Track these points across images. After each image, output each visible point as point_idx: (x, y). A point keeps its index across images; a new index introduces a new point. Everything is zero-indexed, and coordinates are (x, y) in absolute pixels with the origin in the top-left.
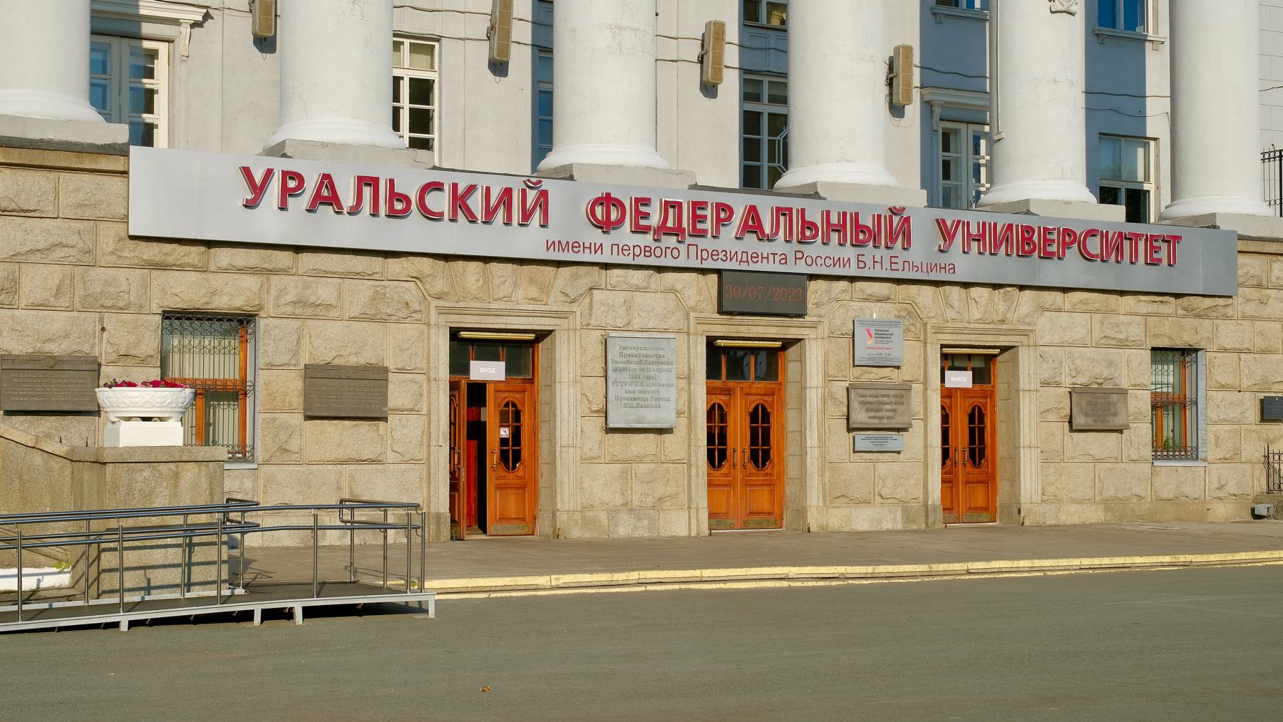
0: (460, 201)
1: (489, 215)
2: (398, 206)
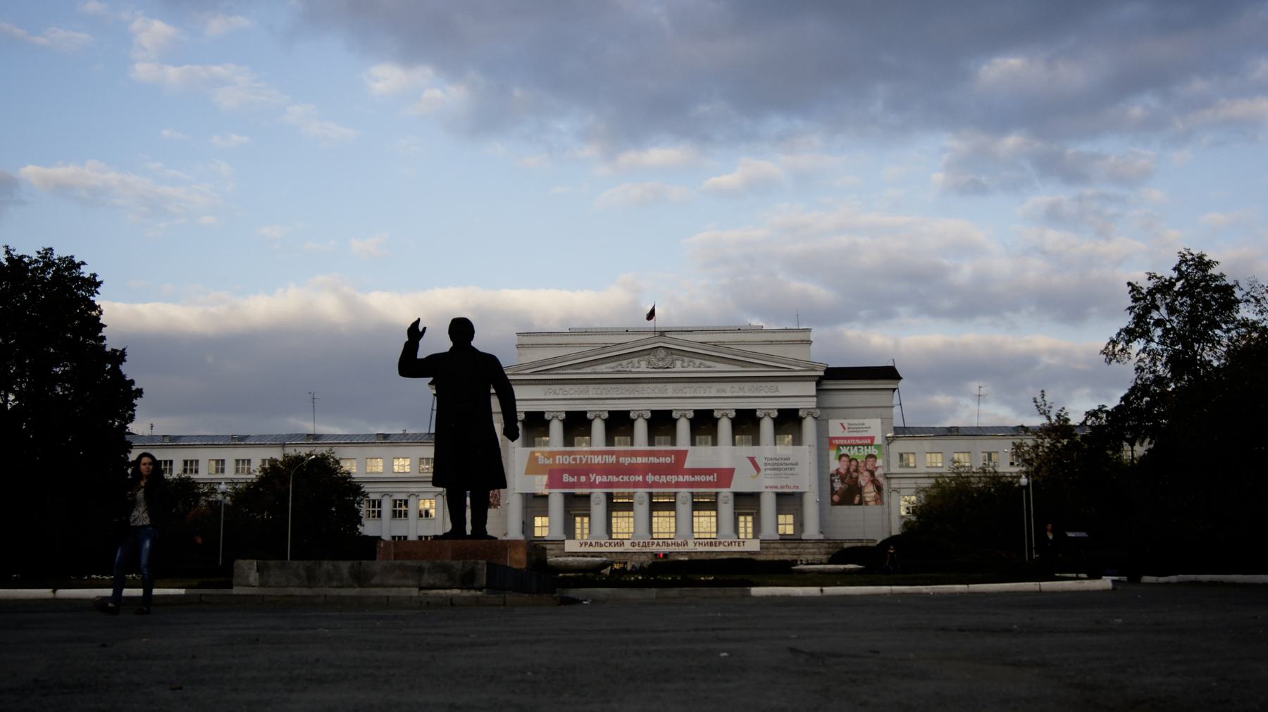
0: (610, 544)
1: (615, 546)
2: (601, 545)
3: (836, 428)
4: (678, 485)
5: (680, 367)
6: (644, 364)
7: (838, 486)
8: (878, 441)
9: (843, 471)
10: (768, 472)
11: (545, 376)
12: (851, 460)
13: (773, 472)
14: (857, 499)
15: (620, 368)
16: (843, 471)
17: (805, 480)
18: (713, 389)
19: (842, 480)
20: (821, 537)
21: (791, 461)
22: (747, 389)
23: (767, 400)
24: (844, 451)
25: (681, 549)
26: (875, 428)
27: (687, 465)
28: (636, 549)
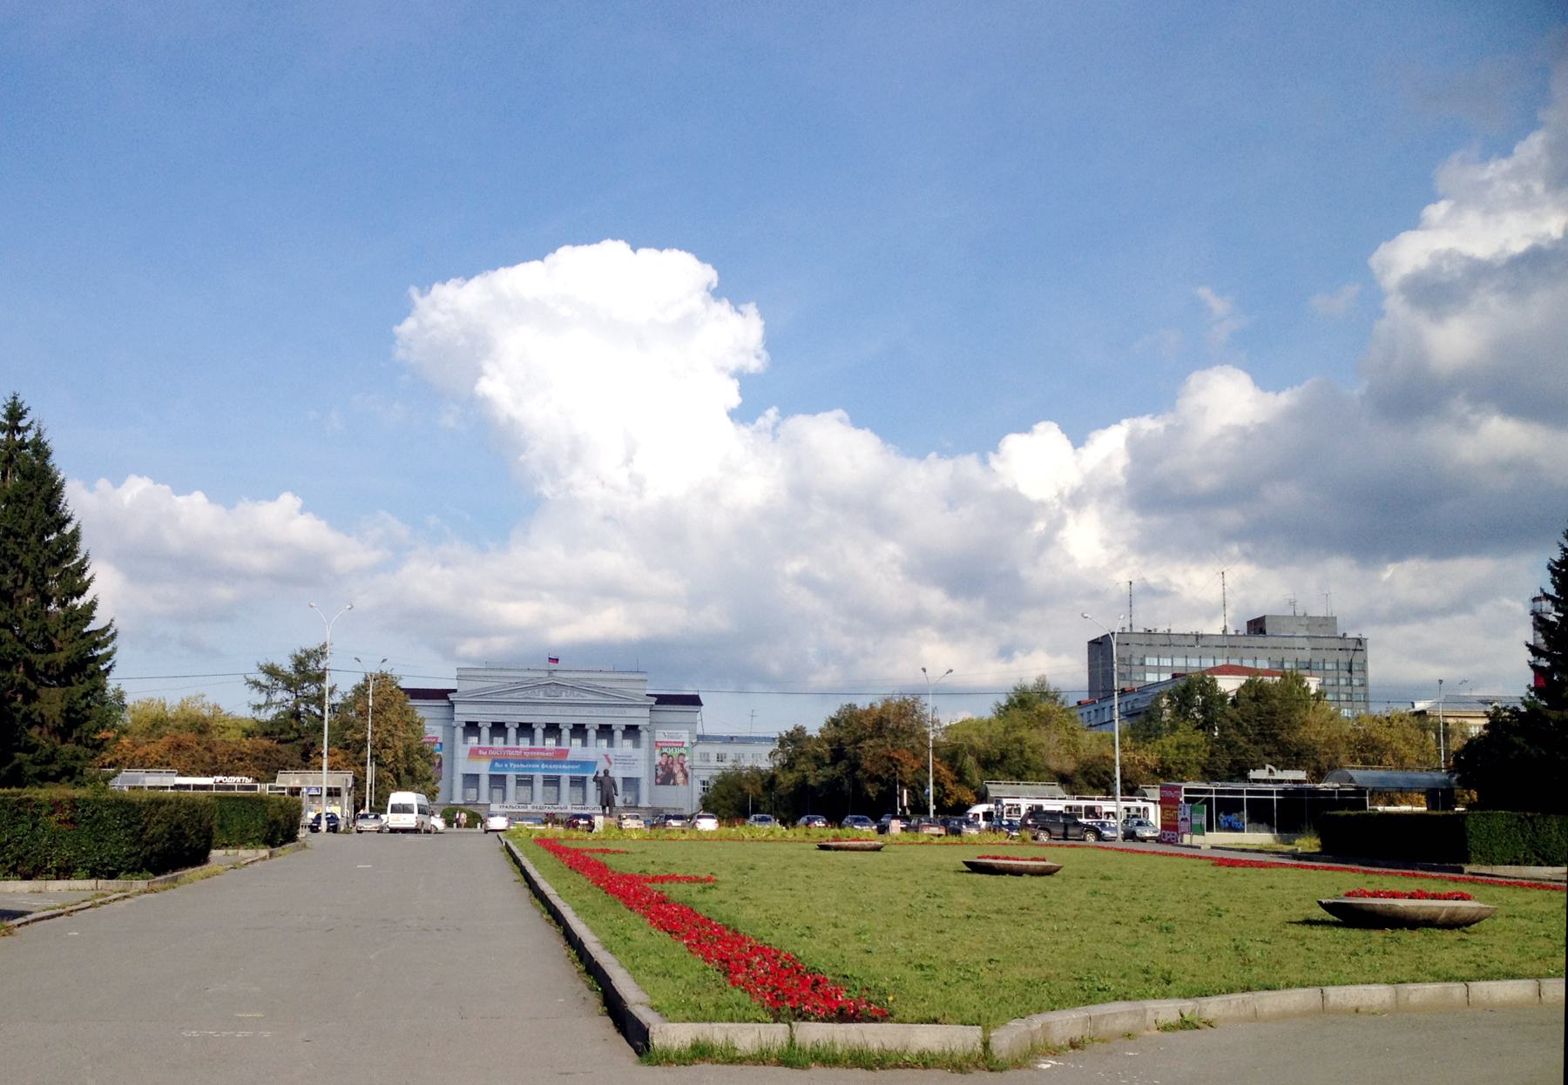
2: (513, 808)
3: (660, 736)
4: (562, 770)
5: (565, 696)
6: (541, 693)
7: (660, 772)
8: (686, 745)
9: (663, 763)
10: (617, 765)
11: (479, 699)
12: (668, 757)
13: (622, 765)
14: (672, 781)
15: (526, 696)
16: (663, 763)
17: (642, 771)
18: (585, 711)
19: (663, 769)
20: (650, 806)
21: (634, 758)
22: (607, 711)
23: (618, 720)
24: (665, 750)
25: (563, 811)
26: (685, 736)
27: (569, 758)
28: (535, 811)
